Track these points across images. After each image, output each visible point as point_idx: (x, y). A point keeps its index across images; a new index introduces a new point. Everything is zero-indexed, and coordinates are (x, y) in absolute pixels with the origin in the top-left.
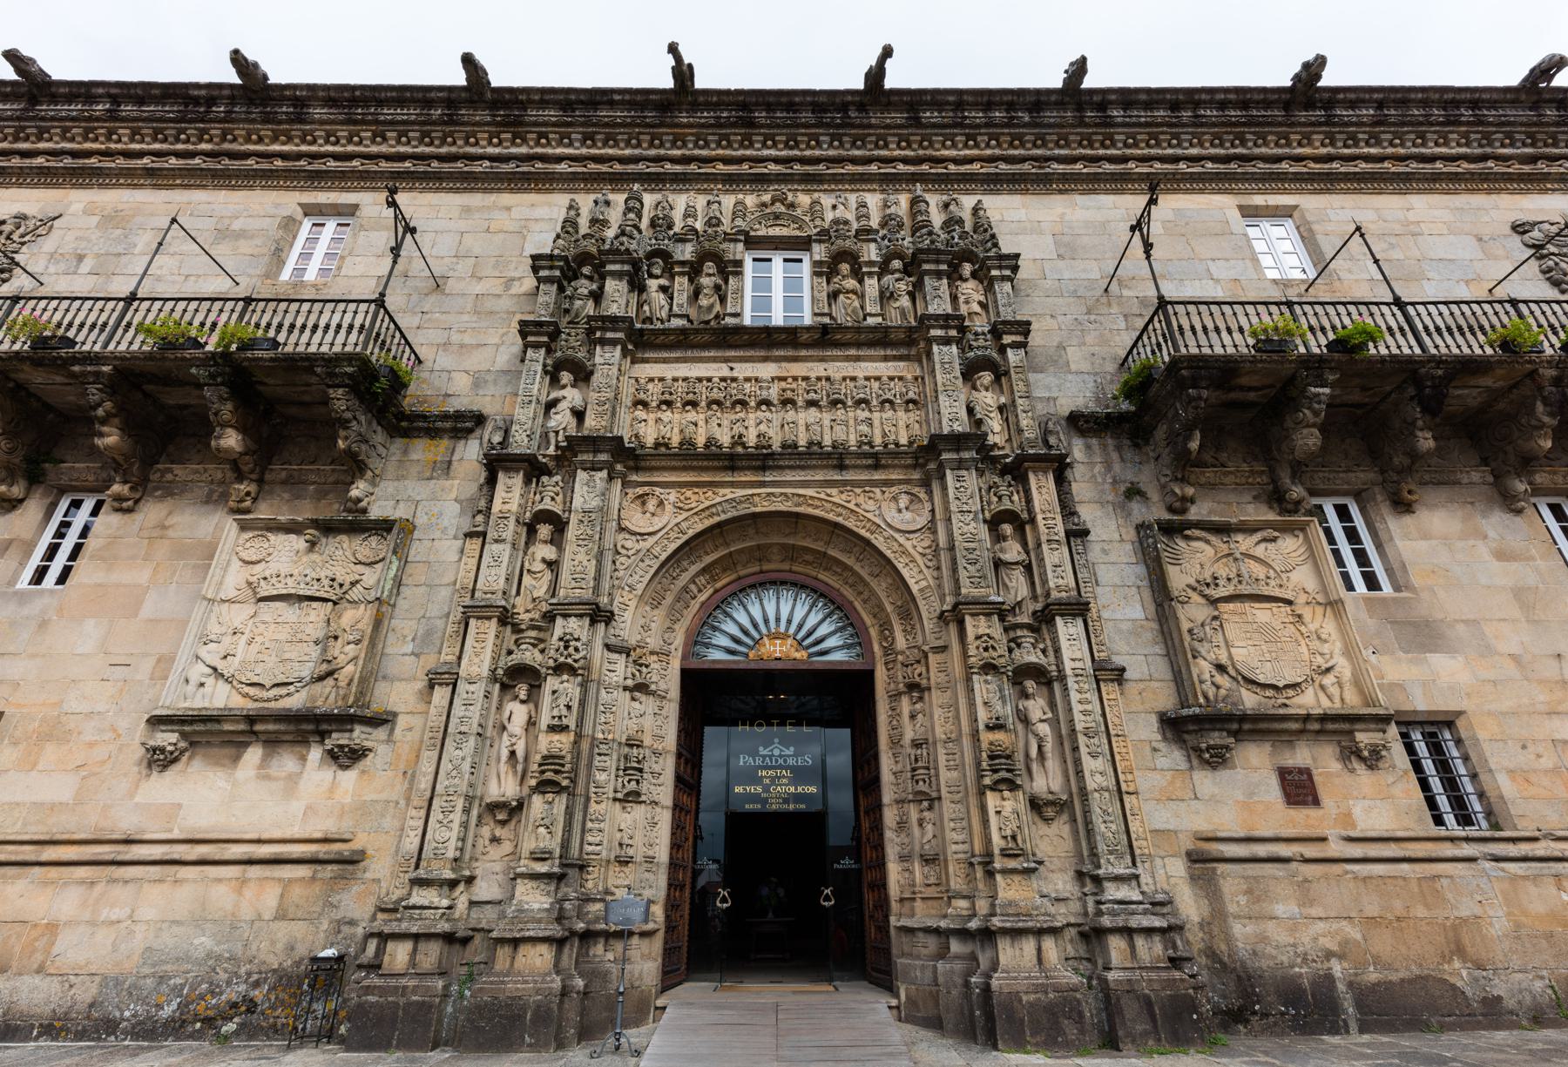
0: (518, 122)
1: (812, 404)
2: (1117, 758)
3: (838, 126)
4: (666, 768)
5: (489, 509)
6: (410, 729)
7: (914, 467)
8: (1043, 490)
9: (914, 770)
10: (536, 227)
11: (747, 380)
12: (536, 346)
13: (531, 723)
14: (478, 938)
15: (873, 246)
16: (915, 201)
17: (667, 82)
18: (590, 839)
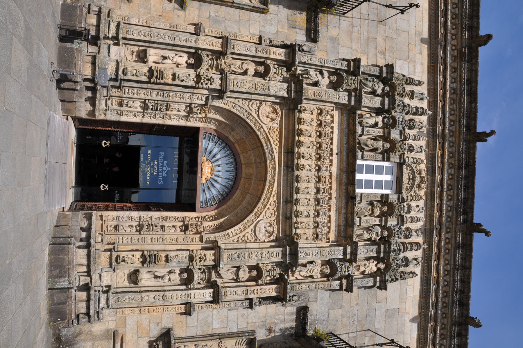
0: (462, 59)
1: (318, 191)
2: (155, 308)
3: (457, 210)
4: (158, 121)
5: (273, 46)
6: (178, 17)
7: (285, 235)
8: (271, 291)
9: (152, 225)
10: (411, 66)
11: (331, 161)
12: (349, 66)
13: (178, 65)
14: (97, 48)
15: (396, 223)
16: (418, 244)
17: (479, 130)
18: (130, 91)
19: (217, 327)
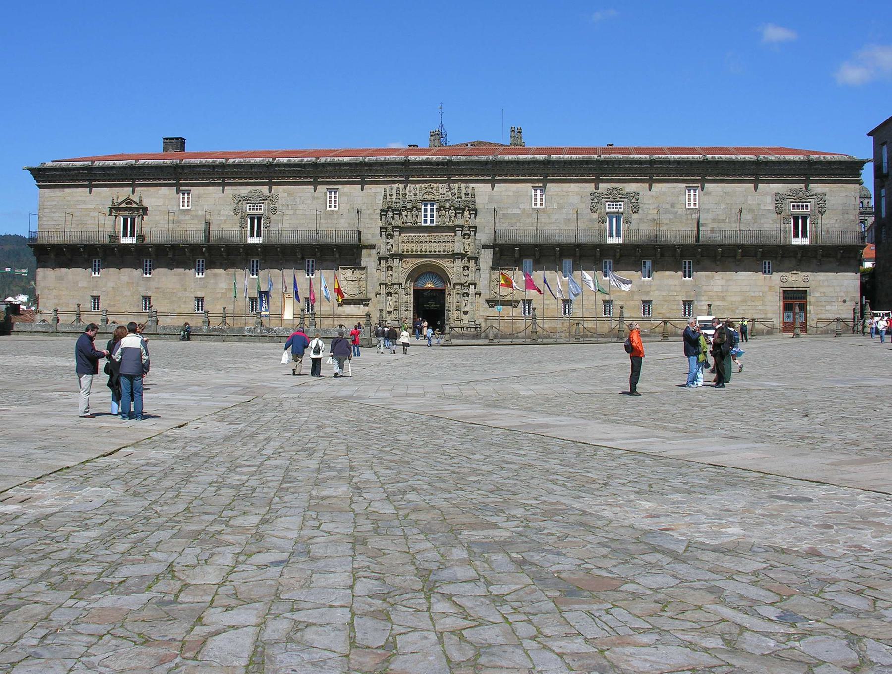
8: (473, 262)
16: (459, 188)
19: (486, 282)
